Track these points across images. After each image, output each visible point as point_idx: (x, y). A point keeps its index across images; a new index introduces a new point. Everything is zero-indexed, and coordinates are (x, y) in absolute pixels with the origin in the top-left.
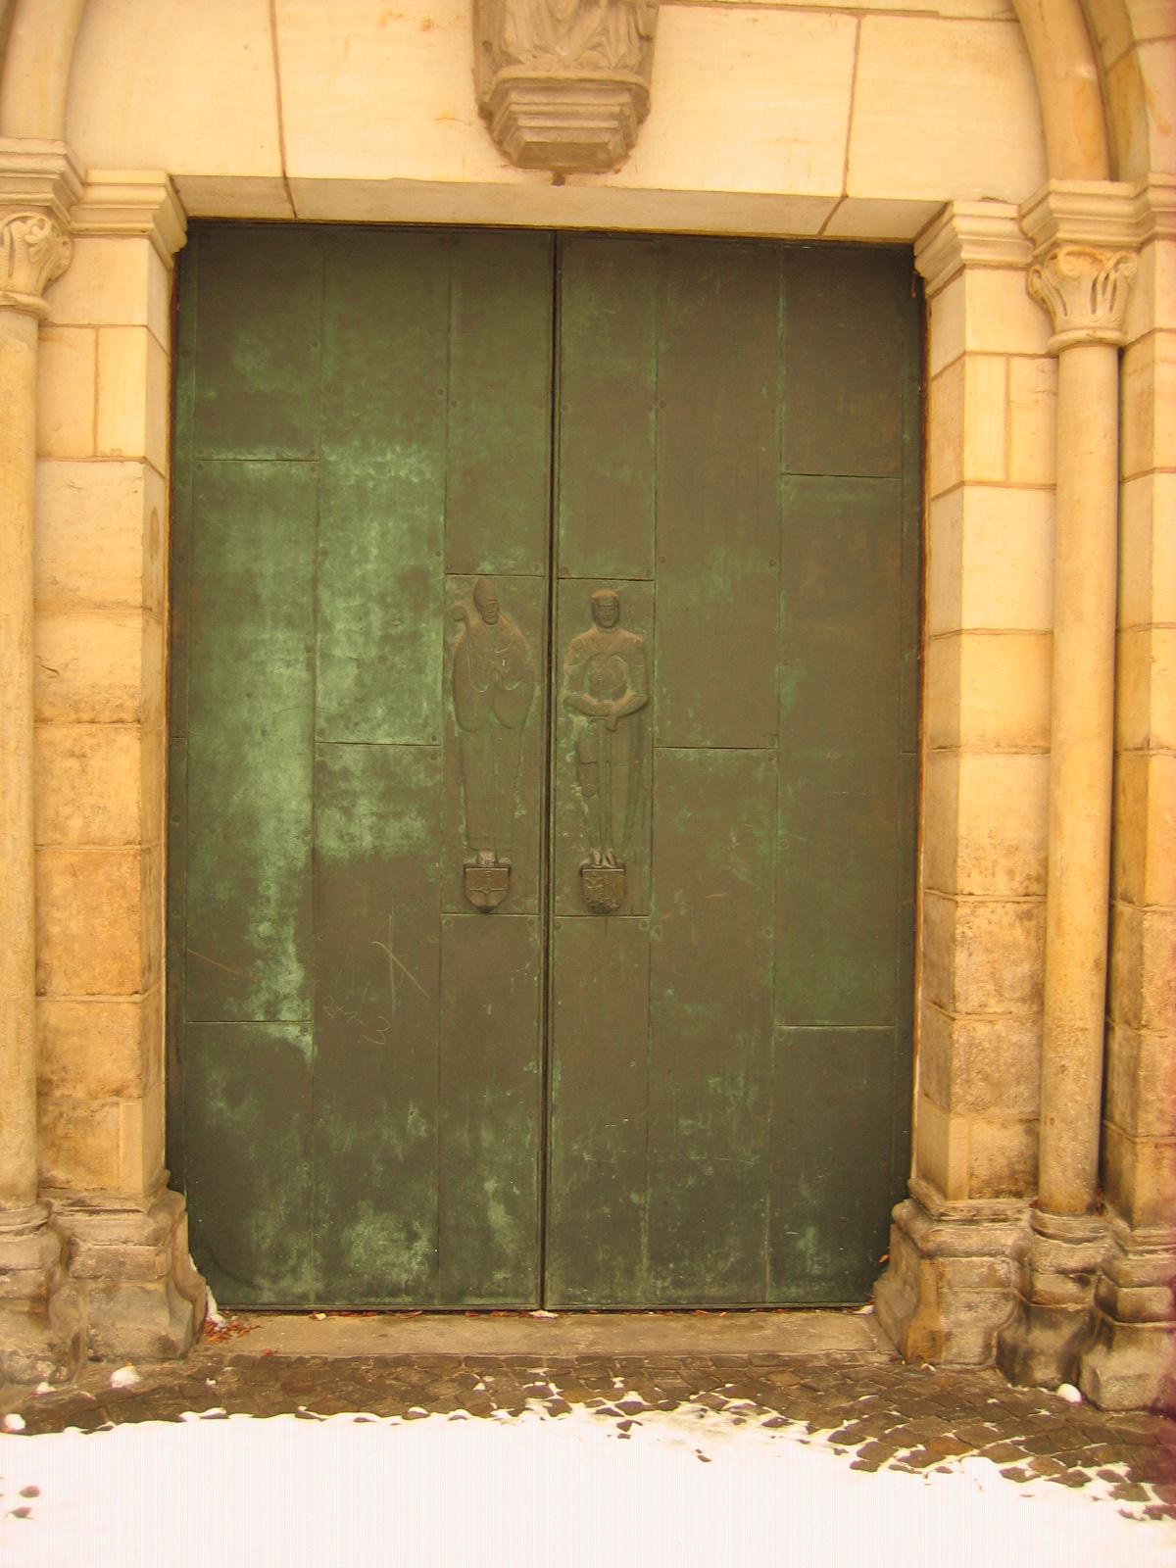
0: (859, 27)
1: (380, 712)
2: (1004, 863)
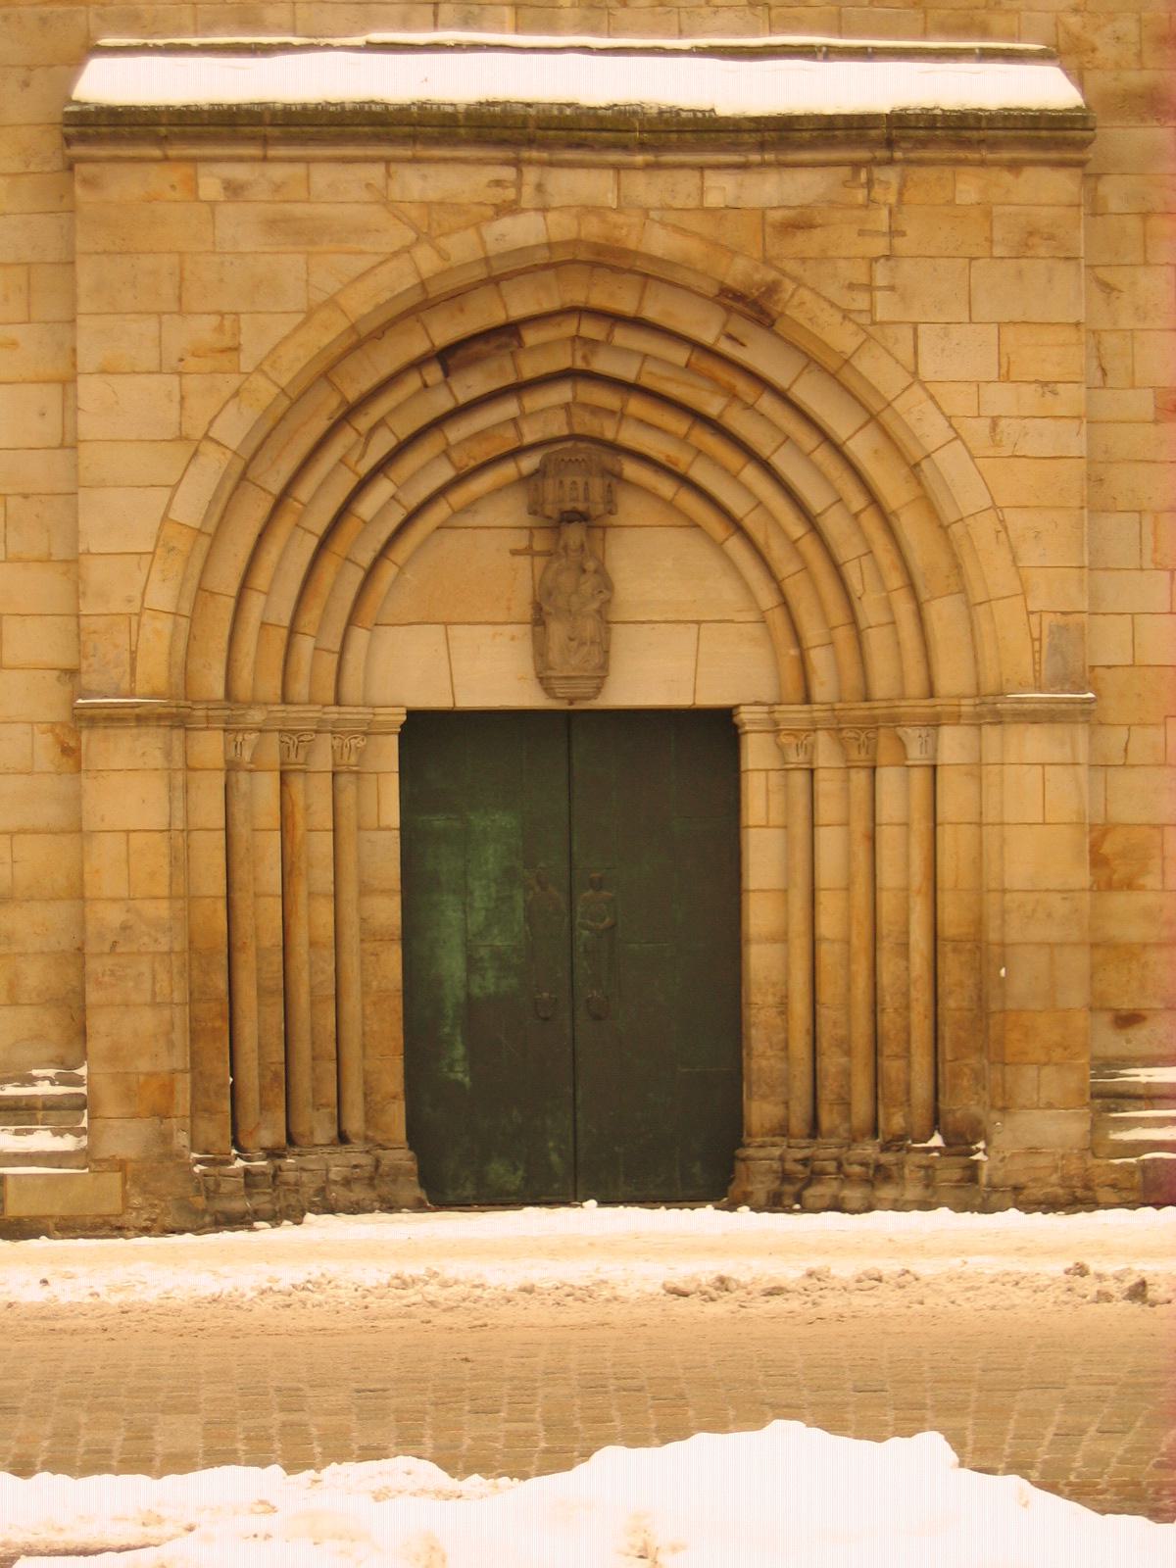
0: (699, 629)
1: (496, 931)
2: (771, 990)
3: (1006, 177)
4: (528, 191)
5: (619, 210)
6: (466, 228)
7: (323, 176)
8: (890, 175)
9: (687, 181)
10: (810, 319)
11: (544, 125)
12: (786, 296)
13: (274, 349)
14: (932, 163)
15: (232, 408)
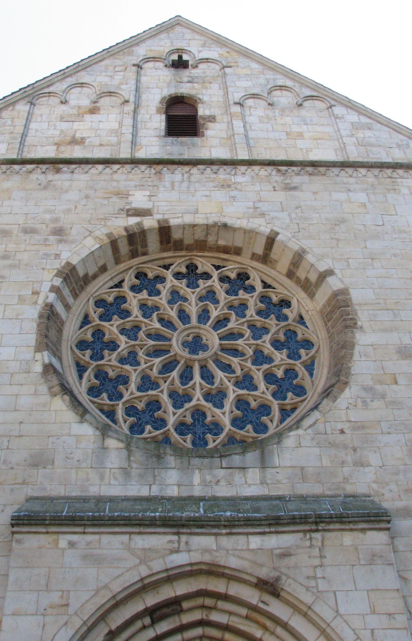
3: (361, 535)
4: (182, 544)
5: (217, 551)
6: (159, 558)
7: (106, 539)
8: (317, 535)
9: (242, 539)
10: (294, 591)
11: (188, 519)
12: (283, 582)
13: (83, 605)
14: (333, 530)
15: (63, 630)
